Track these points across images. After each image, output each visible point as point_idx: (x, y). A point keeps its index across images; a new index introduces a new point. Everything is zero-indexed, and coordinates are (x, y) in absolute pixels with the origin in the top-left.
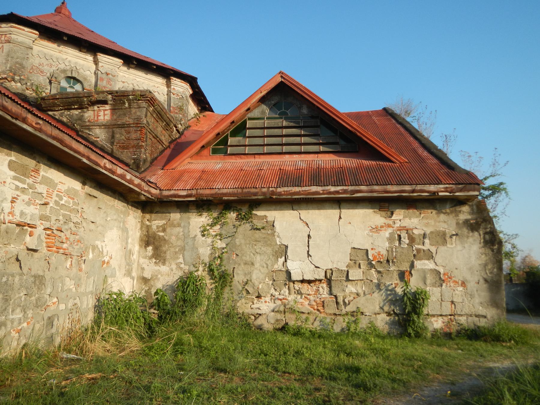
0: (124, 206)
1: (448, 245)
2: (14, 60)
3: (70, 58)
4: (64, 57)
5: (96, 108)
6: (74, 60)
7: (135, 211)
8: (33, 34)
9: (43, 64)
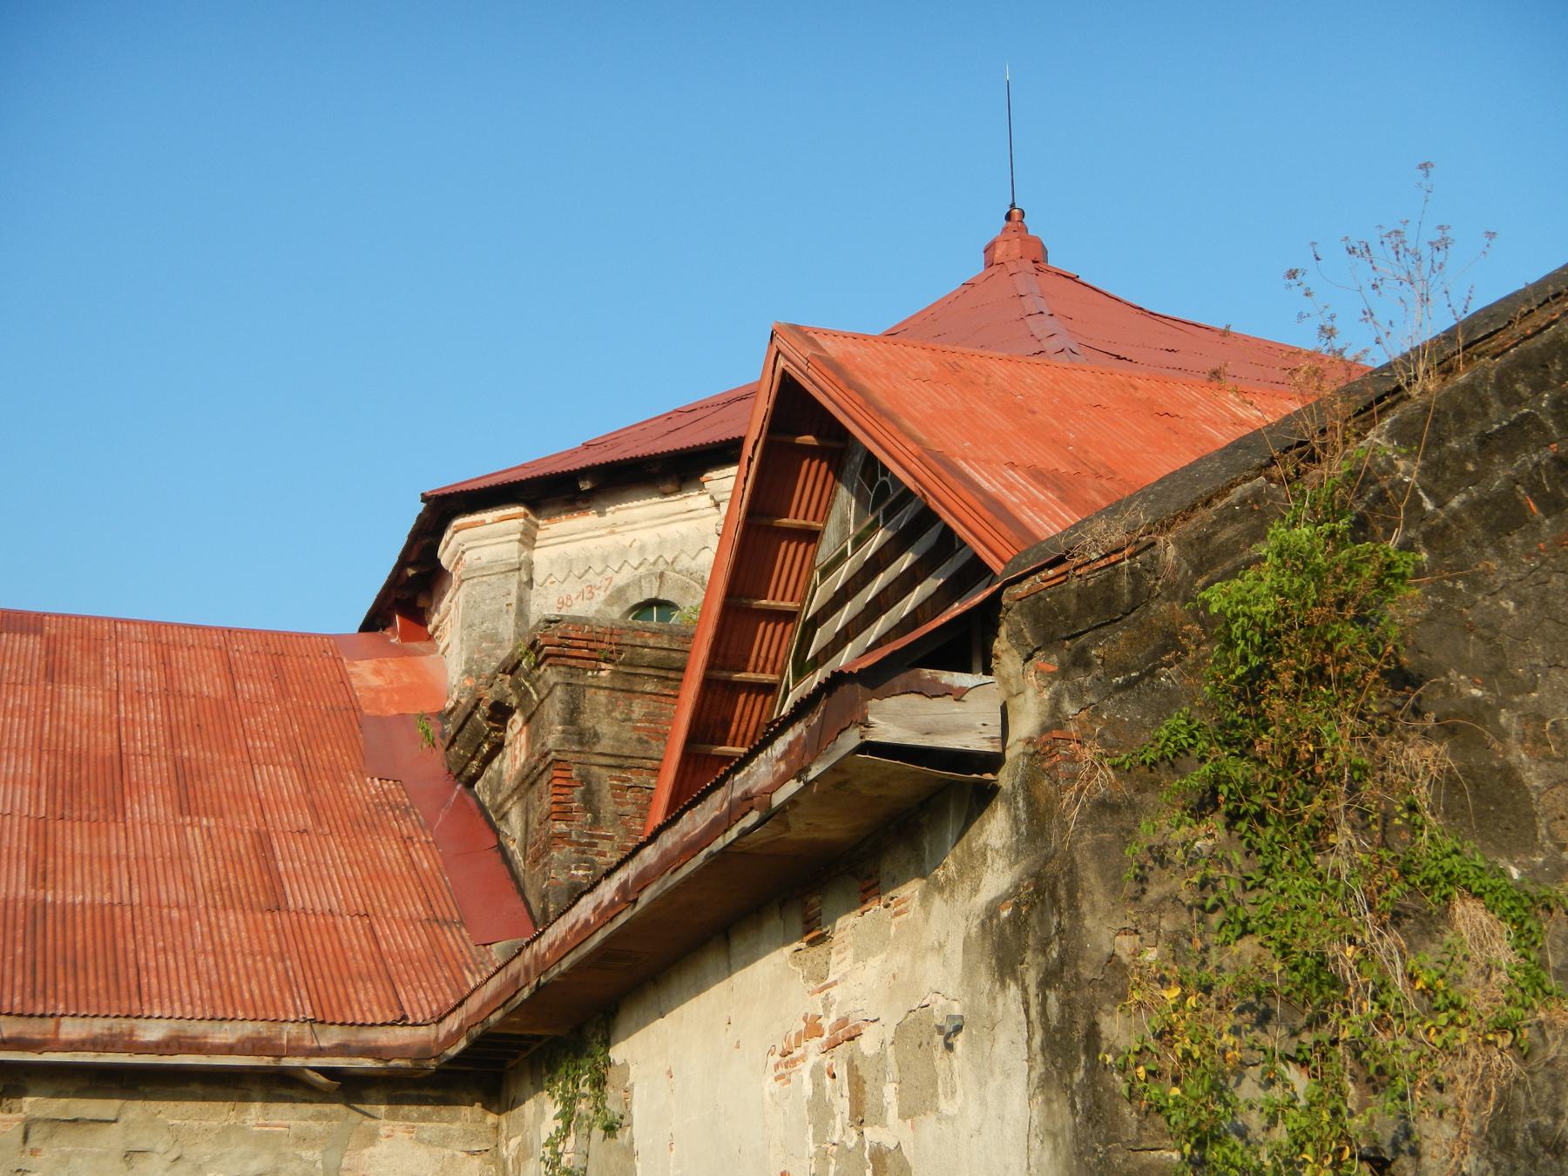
0: (317, 1117)
1: (943, 1105)
4: (626, 540)
5: (510, 734)
6: (647, 536)
8: (503, 523)
9: (569, 598)
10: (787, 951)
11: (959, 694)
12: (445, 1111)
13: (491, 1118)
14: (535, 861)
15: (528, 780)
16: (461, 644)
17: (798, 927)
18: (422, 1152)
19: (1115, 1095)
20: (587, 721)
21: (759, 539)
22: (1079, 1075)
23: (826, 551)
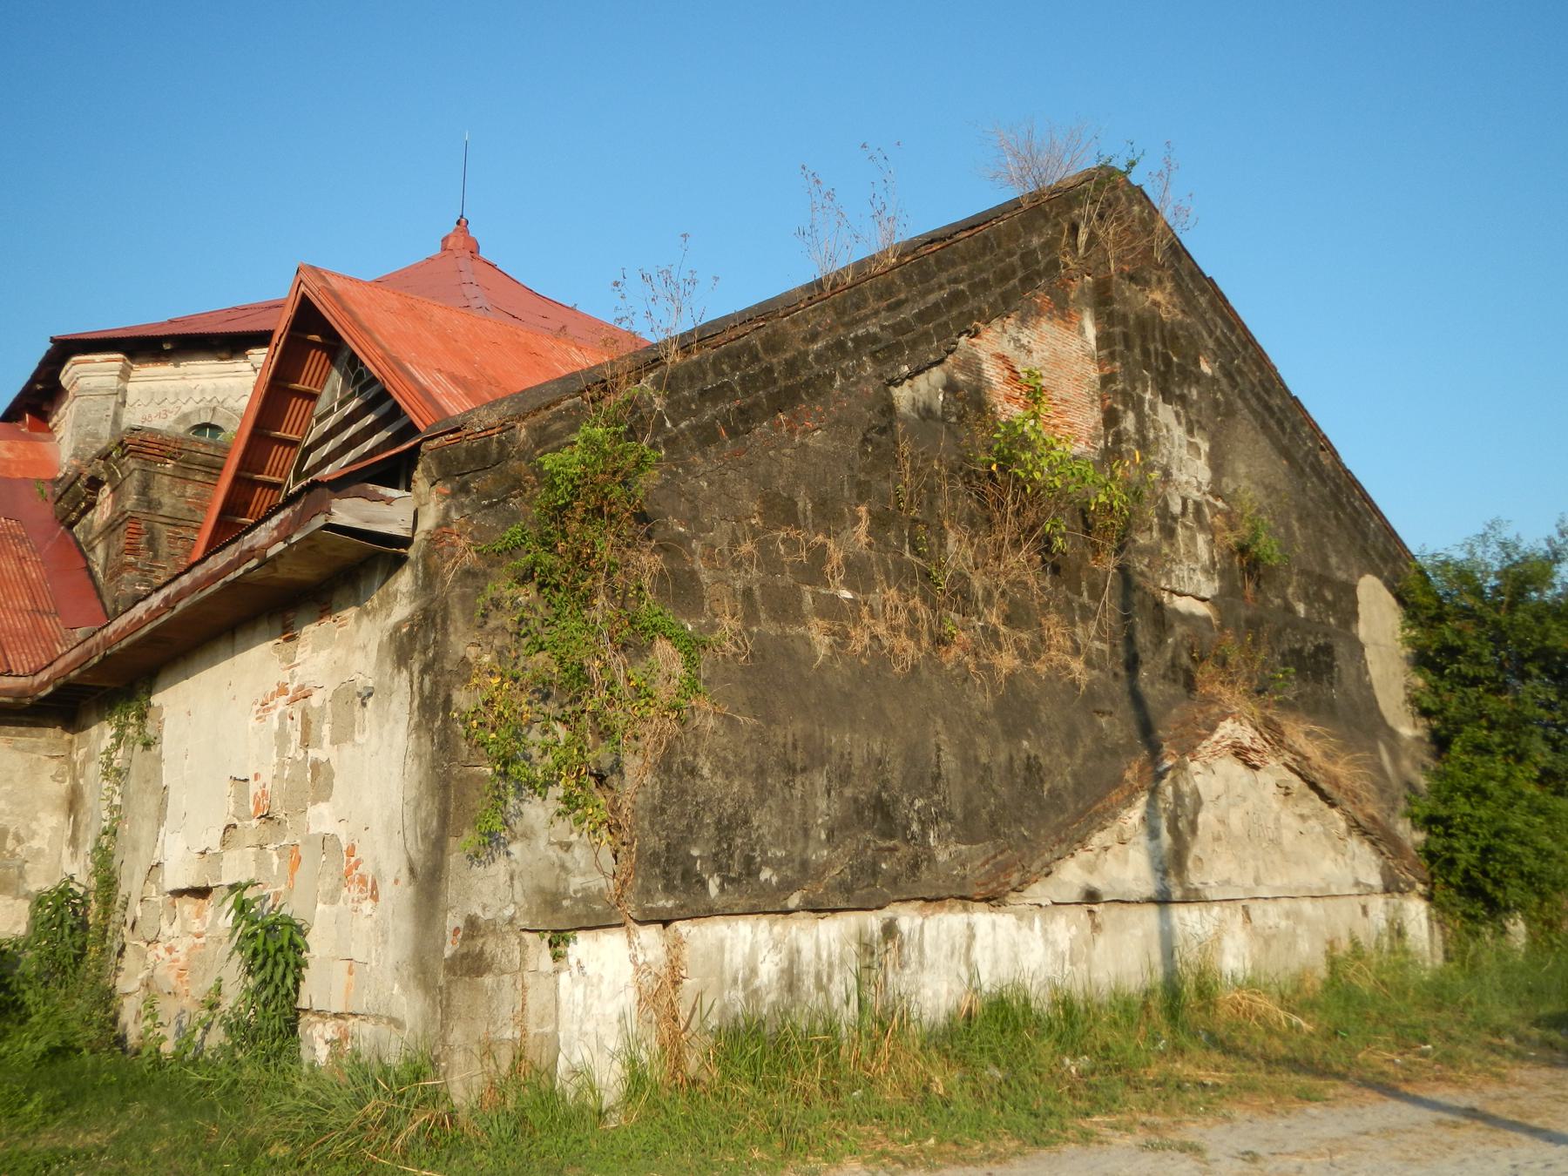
1: (357, 737)
2: (82, 432)
3: (207, 384)
5: (101, 498)
7: (20, 734)
10: (271, 644)
11: (389, 501)
12: (35, 731)
13: (67, 736)
14: (111, 579)
15: (111, 528)
16: (69, 438)
17: (279, 629)
18: (16, 756)
19: (456, 735)
20: (154, 494)
21: (279, 394)
22: (438, 723)
23: (321, 407)
